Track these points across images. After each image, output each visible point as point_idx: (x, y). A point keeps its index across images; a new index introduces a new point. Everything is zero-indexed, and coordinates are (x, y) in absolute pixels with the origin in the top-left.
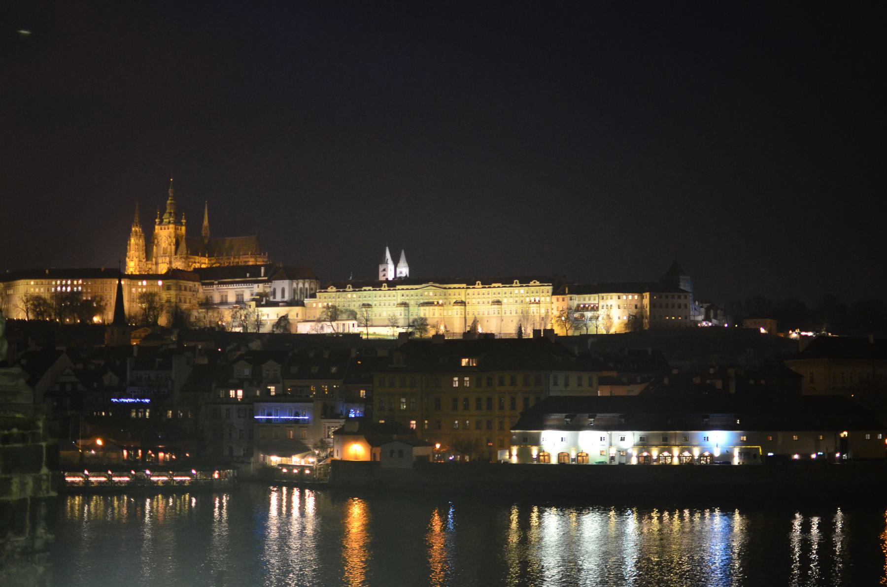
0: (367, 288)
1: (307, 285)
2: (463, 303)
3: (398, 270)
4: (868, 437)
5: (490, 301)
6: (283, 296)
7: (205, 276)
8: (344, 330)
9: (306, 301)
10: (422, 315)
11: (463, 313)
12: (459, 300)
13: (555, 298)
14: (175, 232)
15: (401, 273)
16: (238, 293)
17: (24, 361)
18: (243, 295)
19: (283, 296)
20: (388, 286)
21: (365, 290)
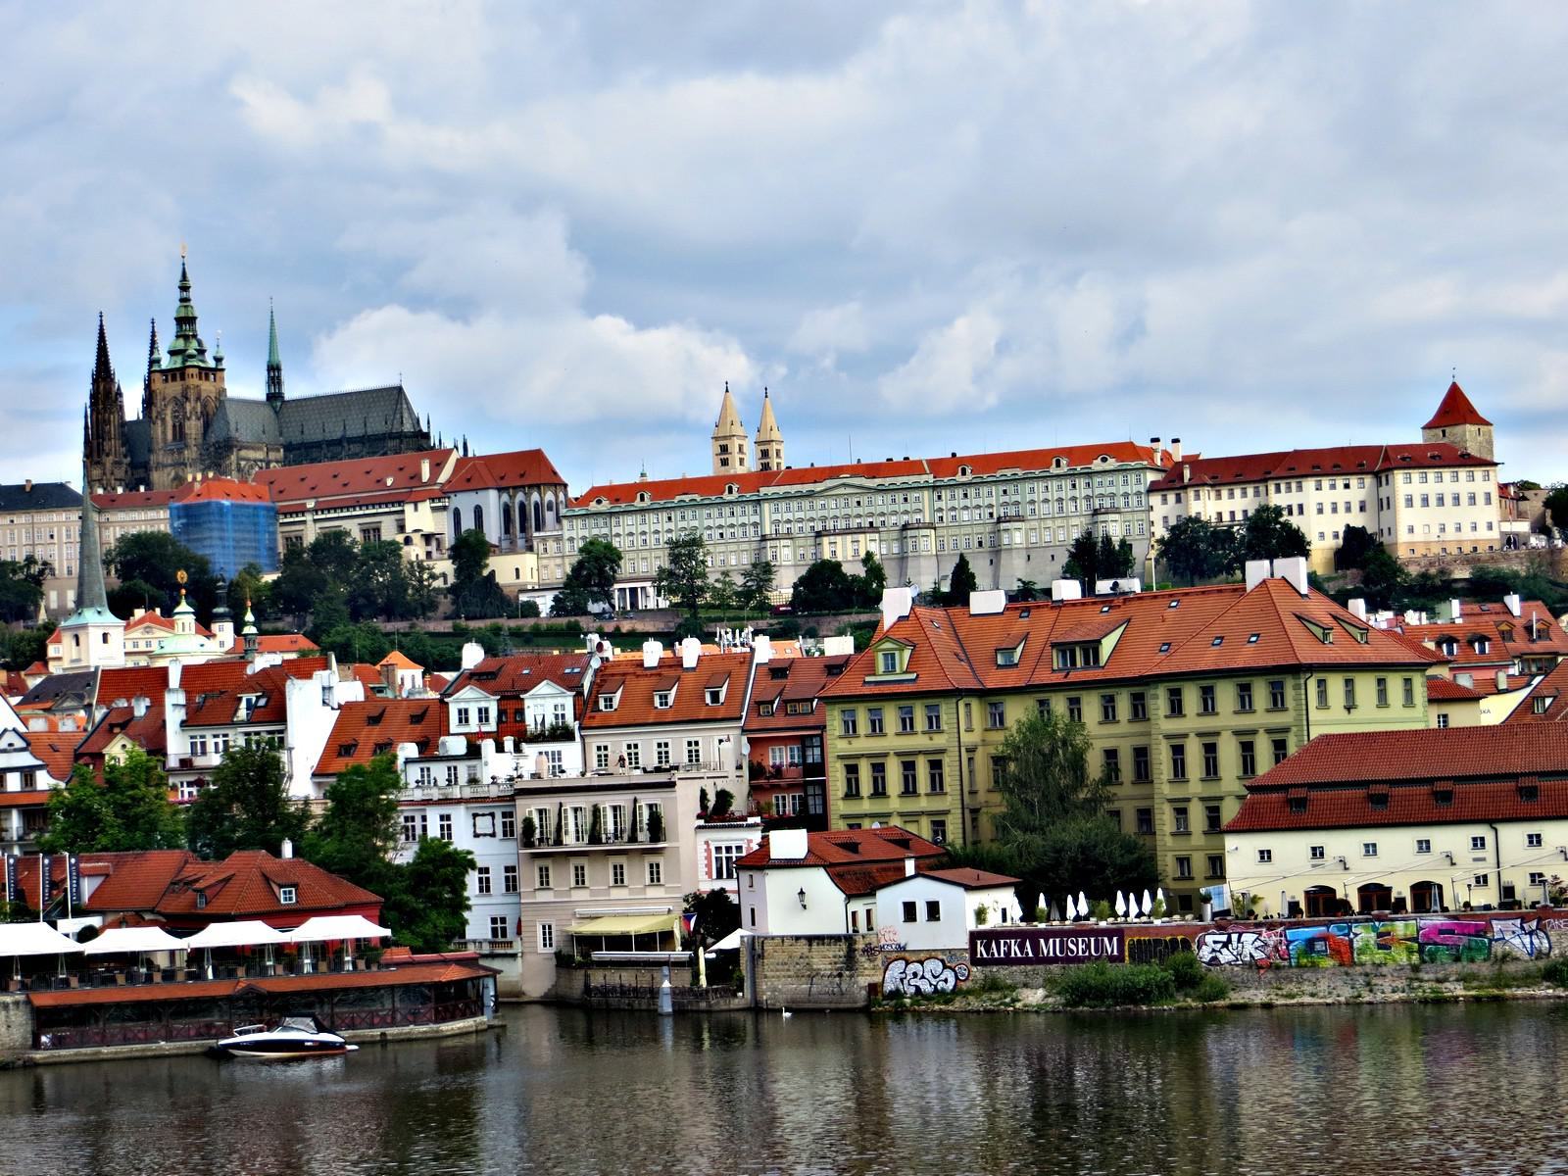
0: (687, 498)
1: (535, 497)
18: (377, 530)
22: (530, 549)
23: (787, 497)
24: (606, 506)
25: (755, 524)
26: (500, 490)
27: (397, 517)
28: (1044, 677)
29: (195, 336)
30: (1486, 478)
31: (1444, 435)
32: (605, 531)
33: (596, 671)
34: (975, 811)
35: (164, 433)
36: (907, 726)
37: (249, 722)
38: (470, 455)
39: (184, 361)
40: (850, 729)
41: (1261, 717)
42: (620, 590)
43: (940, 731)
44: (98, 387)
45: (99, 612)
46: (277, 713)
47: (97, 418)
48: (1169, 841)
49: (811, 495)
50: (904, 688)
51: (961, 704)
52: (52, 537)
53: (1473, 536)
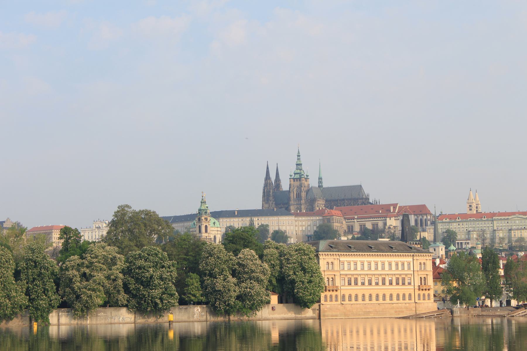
0: (472, 219)
22: (424, 231)
23: (501, 219)
24: (448, 220)
25: (492, 226)
26: (414, 215)
27: (385, 221)
32: (448, 227)
35: (294, 196)
38: (380, 204)
42: (457, 243)
44: (267, 182)
45: (440, 243)
47: (267, 191)
49: (508, 219)
52: (284, 224)
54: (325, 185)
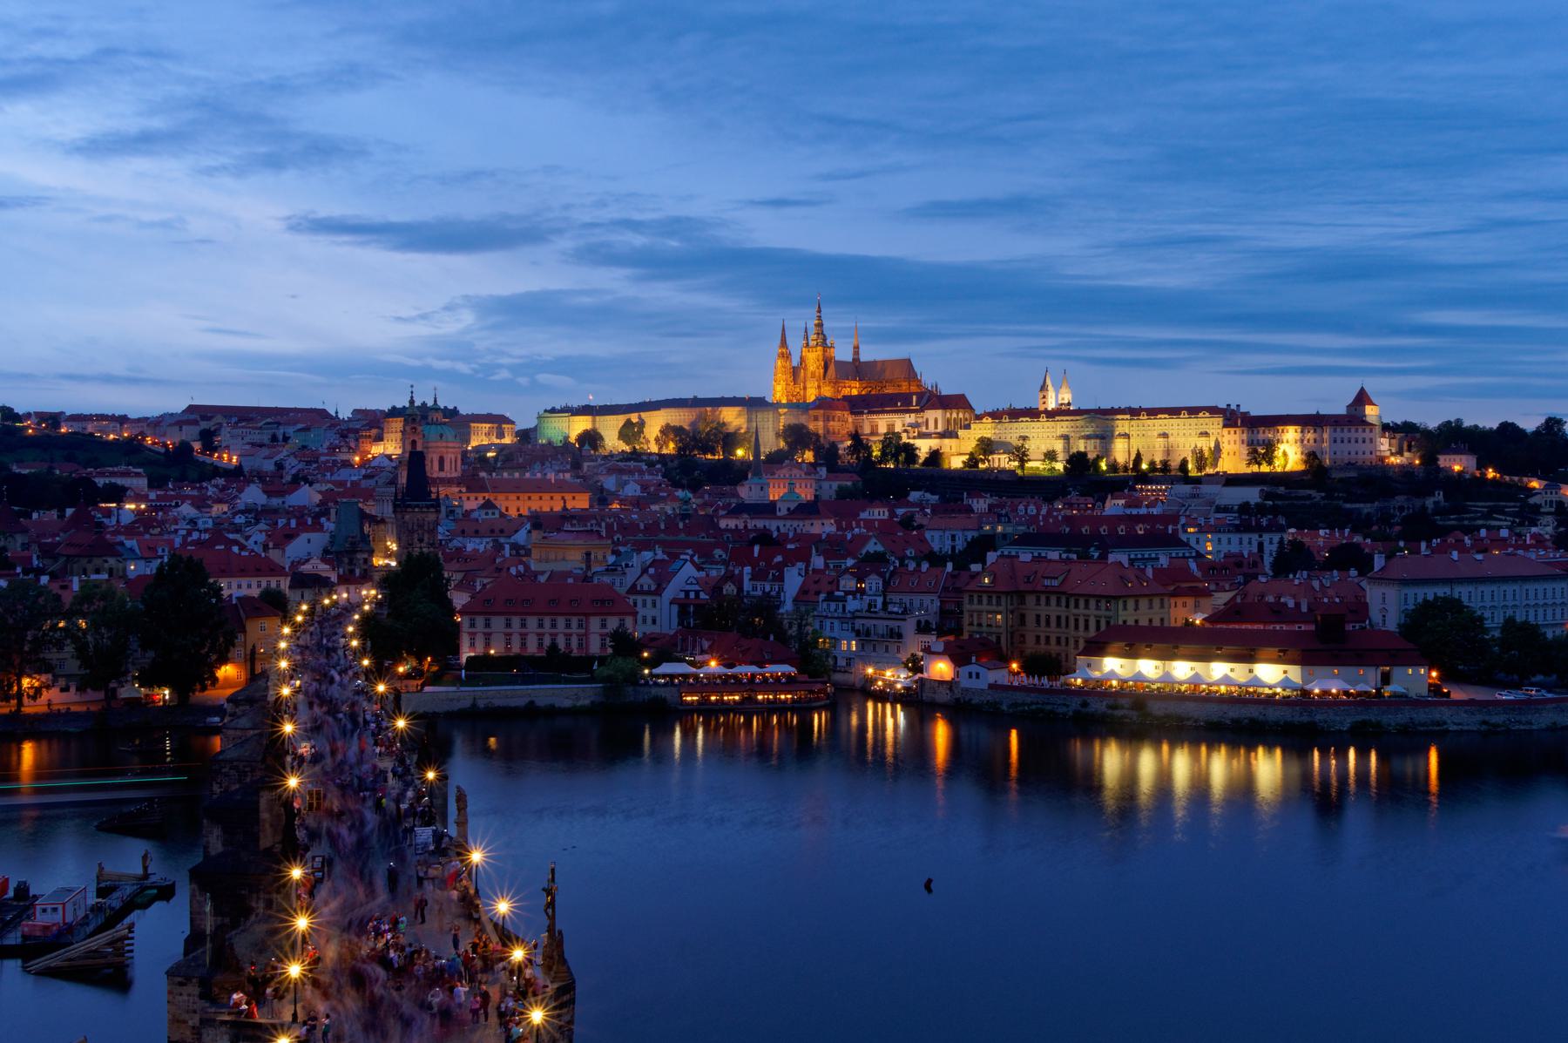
0: (1024, 419)
1: (961, 415)
2: (1127, 436)
3: (1060, 397)
4: (1410, 671)
5: (1156, 434)
6: (936, 427)
7: (858, 405)
8: (999, 465)
9: (961, 433)
10: (1082, 449)
11: (1126, 446)
12: (1123, 432)
13: (1226, 430)
14: (824, 354)
15: (1063, 399)
16: (888, 423)
17: (652, 571)
19: (936, 427)
20: (1047, 417)
21: (1022, 421)
28: (1039, 588)
29: (822, 333)
30: (1371, 431)
31: (1356, 410)
33: (892, 572)
34: (1012, 633)
36: (990, 603)
37: (773, 580)
39: (817, 344)
40: (971, 601)
41: (1103, 612)
43: (1000, 605)
46: (781, 578)
48: (1072, 650)
50: (990, 589)
51: (1009, 598)
53: (1363, 457)
54: (864, 357)
